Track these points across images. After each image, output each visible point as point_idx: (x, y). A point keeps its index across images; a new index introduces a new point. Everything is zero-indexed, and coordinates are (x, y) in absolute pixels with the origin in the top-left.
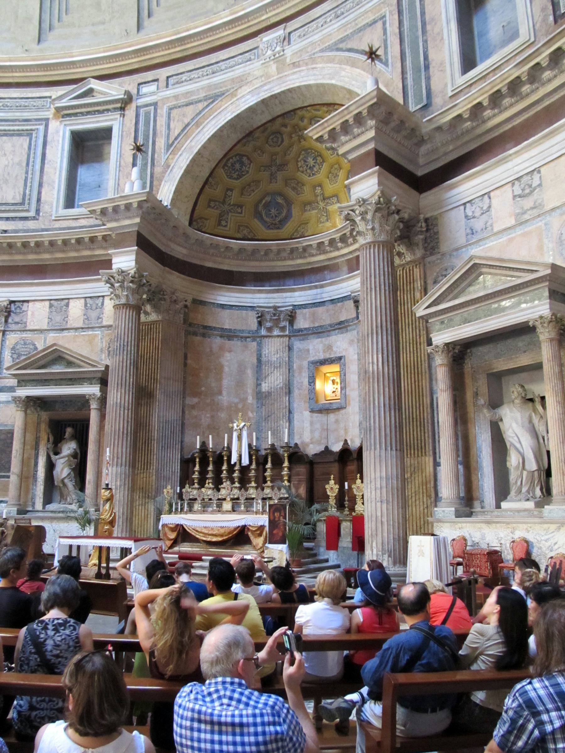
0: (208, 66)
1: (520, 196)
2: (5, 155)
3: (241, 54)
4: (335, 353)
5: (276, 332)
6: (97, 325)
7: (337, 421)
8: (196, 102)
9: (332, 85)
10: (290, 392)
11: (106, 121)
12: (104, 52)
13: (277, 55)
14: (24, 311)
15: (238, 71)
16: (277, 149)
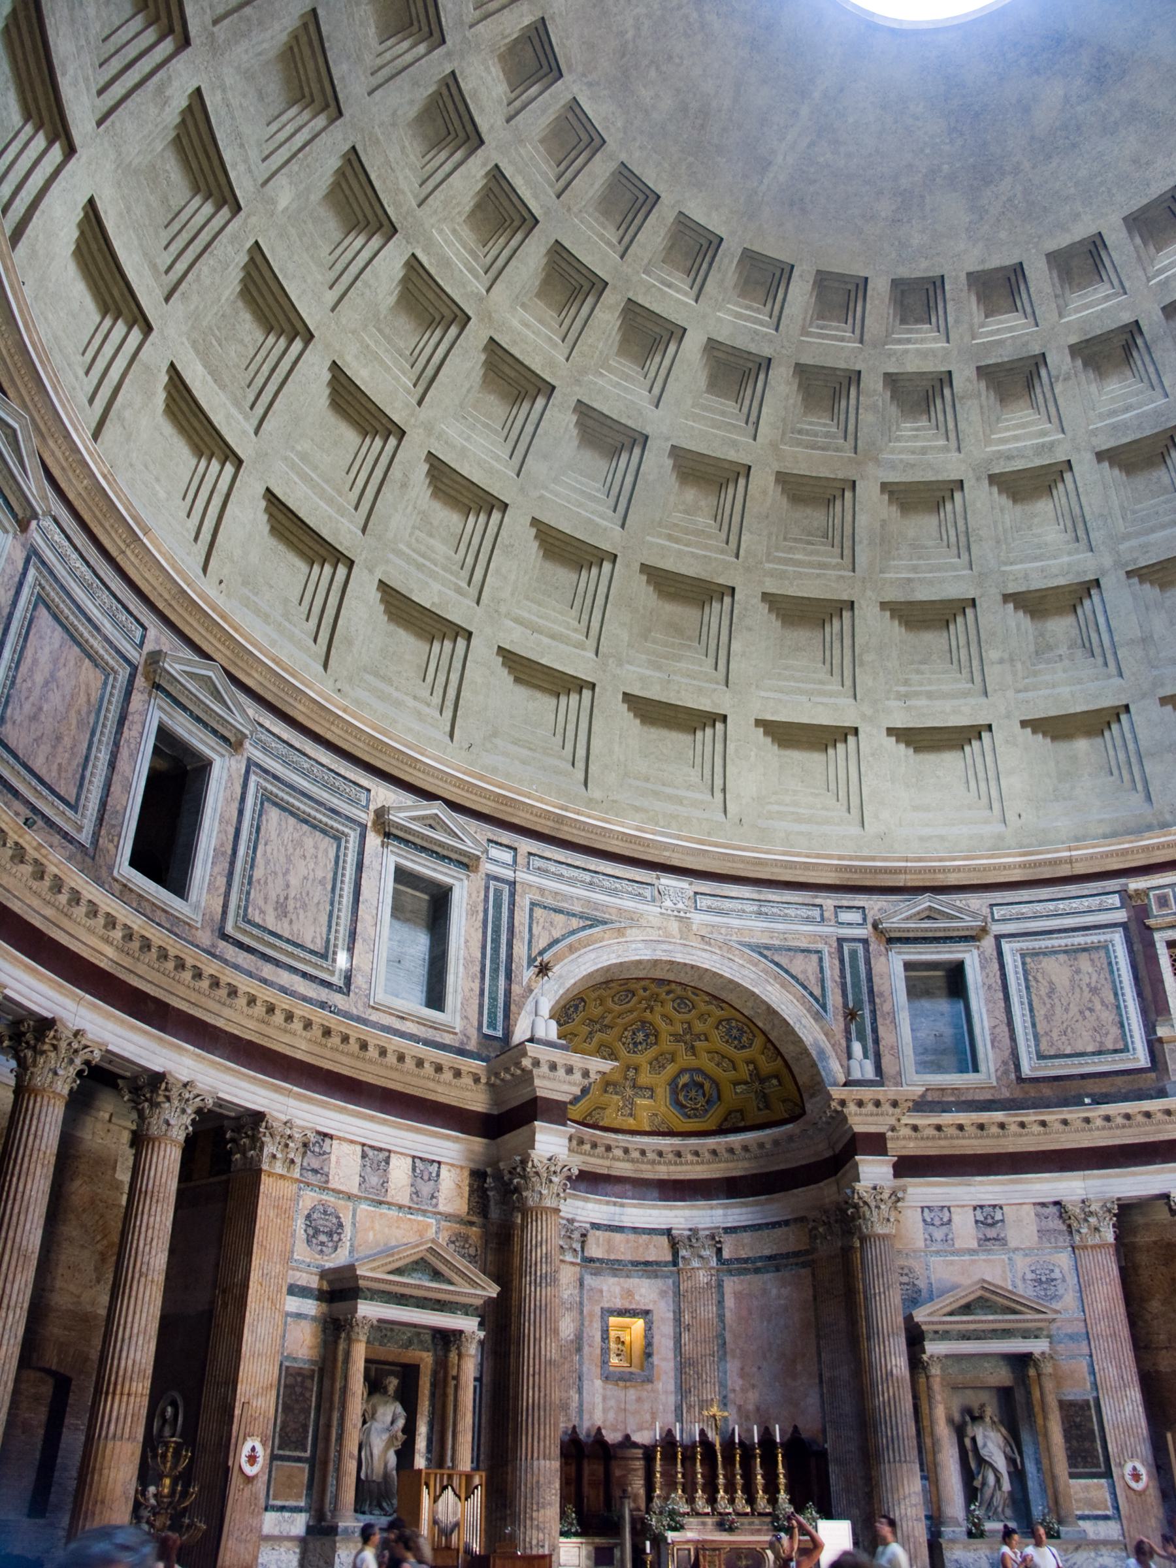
0: (584, 869)
1: (982, 1223)
2: (305, 856)
3: (629, 880)
4: (638, 1303)
5: (569, 1257)
6: (430, 1209)
7: (639, 1400)
8: (568, 914)
9: (753, 994)
10: (579, 1350)
11: (446, 874)
12: (464, 773)
13: (682, 914)
14: (325, 1153)
15: (628, 904)
16: (617, 1007)
